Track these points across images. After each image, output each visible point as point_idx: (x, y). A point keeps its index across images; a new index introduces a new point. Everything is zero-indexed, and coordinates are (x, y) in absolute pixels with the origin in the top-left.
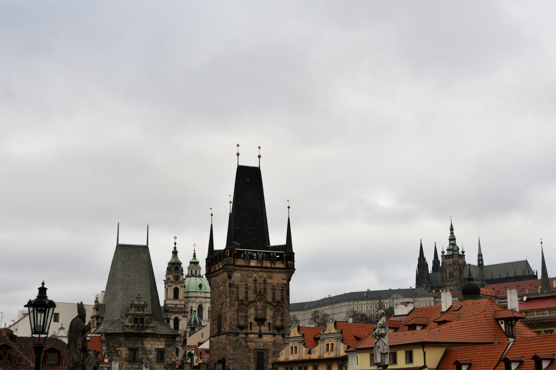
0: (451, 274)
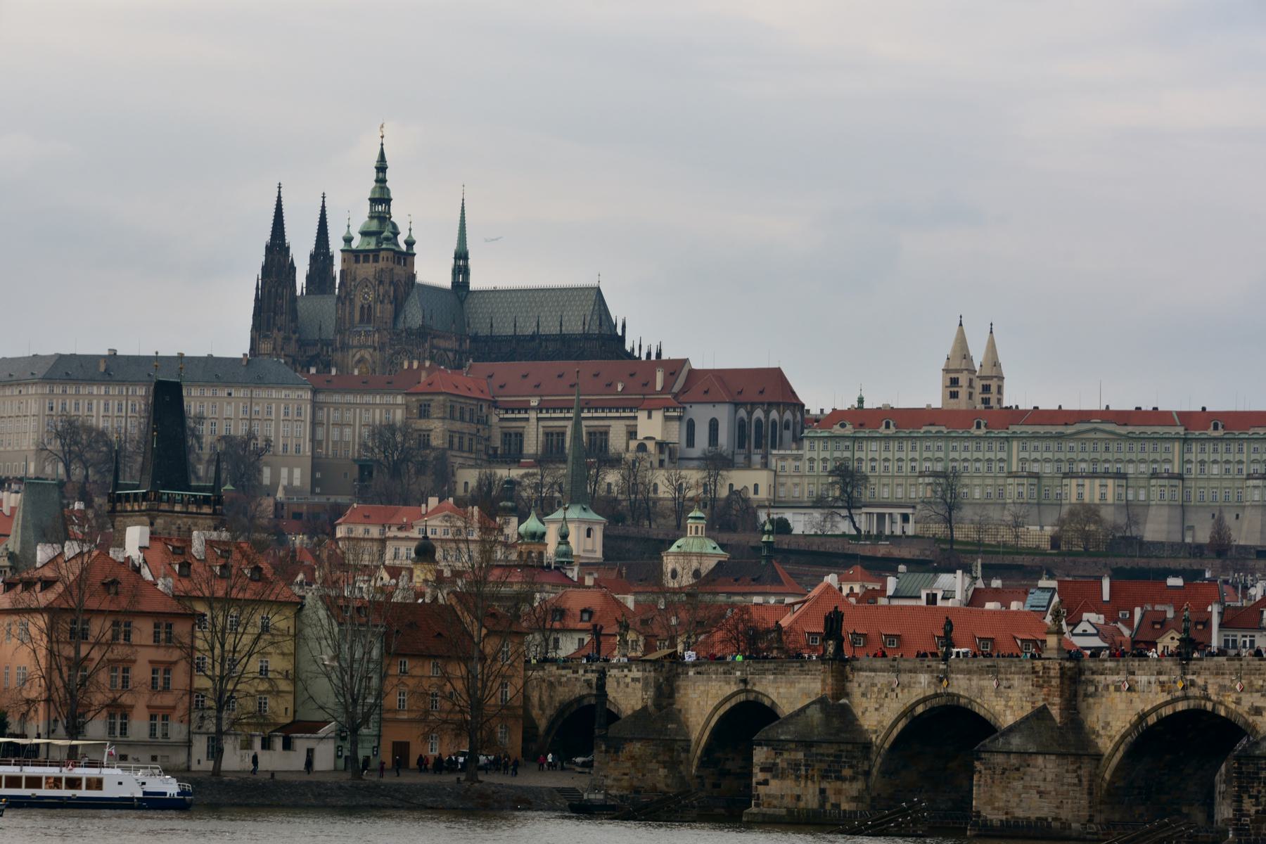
0: (366, 311)
